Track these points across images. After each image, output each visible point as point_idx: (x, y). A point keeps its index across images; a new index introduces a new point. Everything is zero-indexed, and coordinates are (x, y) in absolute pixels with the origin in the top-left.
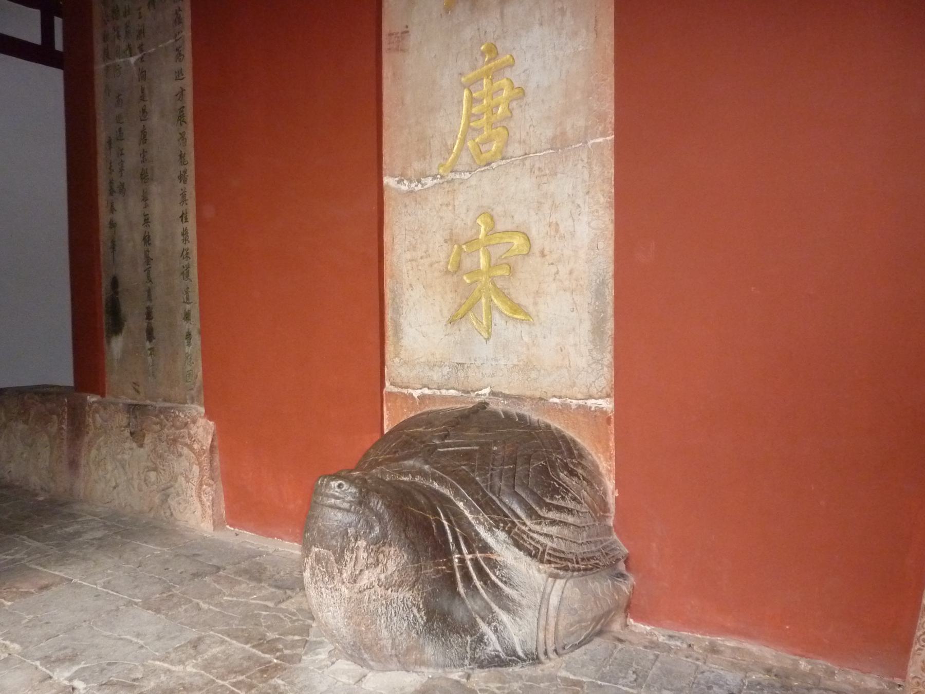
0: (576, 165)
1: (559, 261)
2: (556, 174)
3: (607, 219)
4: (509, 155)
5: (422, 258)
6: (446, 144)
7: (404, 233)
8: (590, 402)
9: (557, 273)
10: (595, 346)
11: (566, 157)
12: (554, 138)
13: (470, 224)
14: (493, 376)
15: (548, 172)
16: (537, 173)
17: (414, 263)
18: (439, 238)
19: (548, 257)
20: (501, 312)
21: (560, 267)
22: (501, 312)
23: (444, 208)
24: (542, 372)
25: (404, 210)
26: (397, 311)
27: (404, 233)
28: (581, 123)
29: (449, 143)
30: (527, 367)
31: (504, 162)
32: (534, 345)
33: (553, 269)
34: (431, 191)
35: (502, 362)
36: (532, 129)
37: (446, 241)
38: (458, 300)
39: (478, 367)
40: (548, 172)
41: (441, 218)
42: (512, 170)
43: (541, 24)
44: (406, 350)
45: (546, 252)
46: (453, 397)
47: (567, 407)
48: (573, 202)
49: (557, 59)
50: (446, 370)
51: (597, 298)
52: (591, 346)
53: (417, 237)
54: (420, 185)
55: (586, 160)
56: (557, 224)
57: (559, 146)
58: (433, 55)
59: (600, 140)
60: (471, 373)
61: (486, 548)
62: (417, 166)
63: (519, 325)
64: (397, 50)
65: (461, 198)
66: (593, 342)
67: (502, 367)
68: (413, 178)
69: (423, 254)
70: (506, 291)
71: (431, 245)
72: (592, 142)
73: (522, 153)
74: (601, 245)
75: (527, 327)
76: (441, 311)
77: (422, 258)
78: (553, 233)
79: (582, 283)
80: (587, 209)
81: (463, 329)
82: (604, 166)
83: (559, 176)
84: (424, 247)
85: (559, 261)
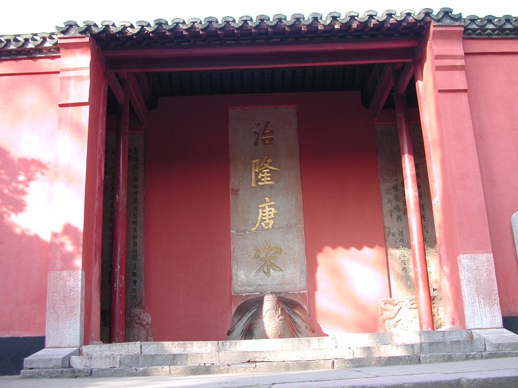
8: (301, 292)
12: (287, 225)
13: (262, 245)
14: (271, 287)
28: (294, 221)
30: (281, 284)
33: (288, 257)
46: (258, 294)
47: (293, 293)
50: (255, 287)
60: (263, 287)
61: (293, 319)
64: (235, 194)
74: (301, 251)
82: (301, 232)
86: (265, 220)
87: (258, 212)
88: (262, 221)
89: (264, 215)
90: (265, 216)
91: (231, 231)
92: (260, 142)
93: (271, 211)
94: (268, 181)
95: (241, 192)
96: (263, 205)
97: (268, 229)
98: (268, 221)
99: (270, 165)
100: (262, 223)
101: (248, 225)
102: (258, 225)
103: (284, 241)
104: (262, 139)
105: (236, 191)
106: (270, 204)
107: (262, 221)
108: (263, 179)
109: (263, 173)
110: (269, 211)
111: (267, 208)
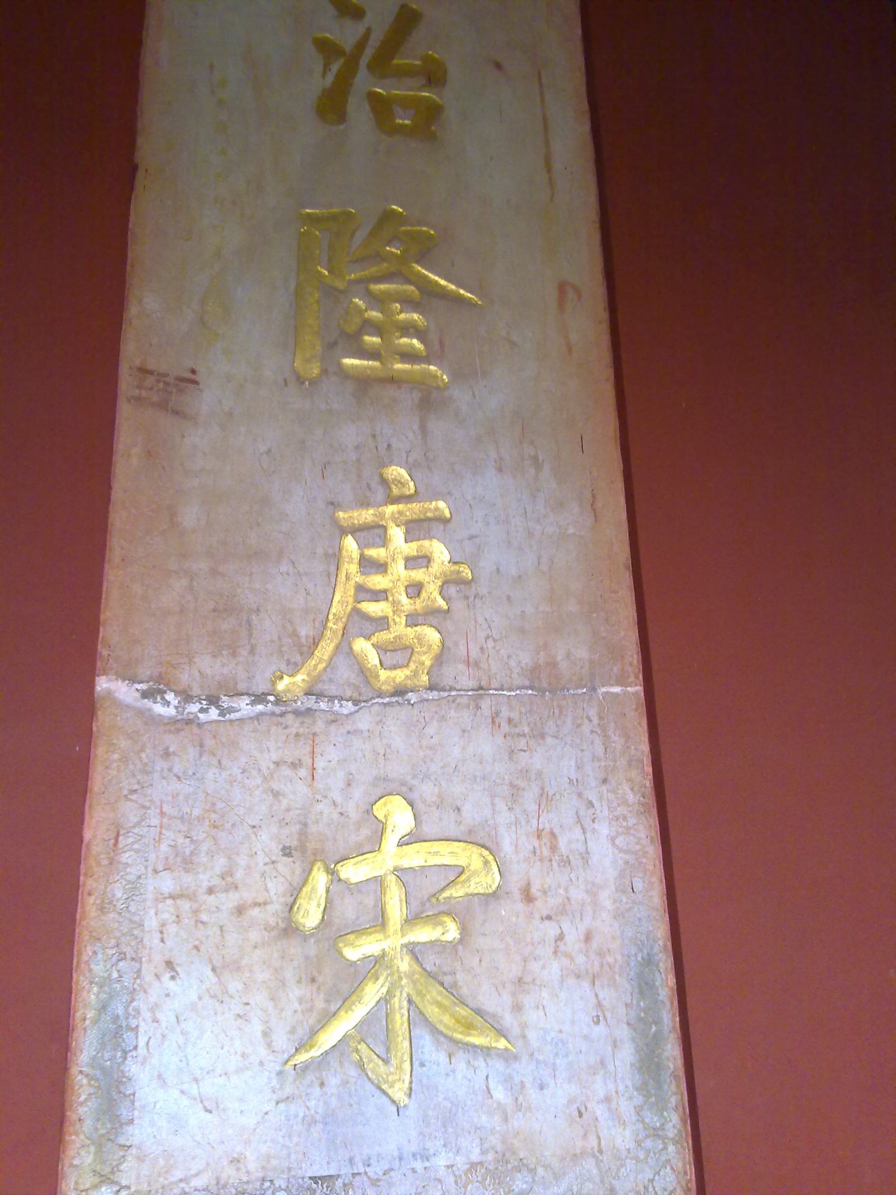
0: (579, 726)
1: (562, 911)
2: (543, 736)
3: (643, 835)
4: (448, 681)
5: (210, 891)
6: (295, 634)
7: (155, 821)
9: (561, 937)
10: (647, 1096)
11: (561, 708)
12: (534, 671)
15: (526, 730)
16: (505, 728)
17: (186, 906)
18: (267, 841)
19: (539, 903)
20: (435, 1031)
21: (566, 926)
22: (435, 1031)
23: (286, 771)
24: (540, 1171)
25: (160, 764)
26: (118, 1036)
27: (155, 821)
29: (303, 632)
31: (433, 695)
32: (518, 1107)
33: (551, 929)
34: (248, 727)
35: (441, 1161)
36: (490, 644)
37: (287, 852)
38: (320, 1004)
39: (375, 1183)
40: (526, 730)
41: (276, 794)
42: (453, 713)
43: (500, 470)
44: (140, 1159)
45: (534, 890)
48: (580, 795)
49: (531, 535)
51: (641, 993)
52: (638, 1100)
53: (199, 833)
54: (214, 713)
55: (596, 721)
56: (553, 834)
57: (545, 685)
58: (263, 449)
59: (617, 689)
62: (209, 666)
63: (480, 1063)
65: (329, 756)
66: (642, 1088)
67: (442, 1173)
68: (196, 691)
69: (216, 881)
70: (447, 979)
71: (242, 860)
72: (604, 690)
73: (472, 684)
75: (499, 1065)
76: (265, 1034)
77: (210, 891)
78: (546, 852)
79: (610, 960)
80: (606, 812)
81: (333, 1081)
82: (627, 737)
83: (549, 740)
84: (221, 863)
85: (562, 911)
86: (382, 623)
87: (335, 557)
88: (360, 623)
89: (378, 582)
90: (379, 595)
91: (103, 684)
92: (359, 113)
93: (422, 560)
94: (409, 356)
95: (208, 399)
96: (367, 515)
97: (400, 692)
98: (399, 628)
99: (425, 251)
100: (361, 645)
101: (252, 651)
102: (326, 649)
103: (515, 792)
104: (373, 98)
105: (175, 390)
106: (413, 509)
107: (360, 623)
108: (373, 340)
109: (379, 301)
110: (411, 562)
111: (396, 534)
